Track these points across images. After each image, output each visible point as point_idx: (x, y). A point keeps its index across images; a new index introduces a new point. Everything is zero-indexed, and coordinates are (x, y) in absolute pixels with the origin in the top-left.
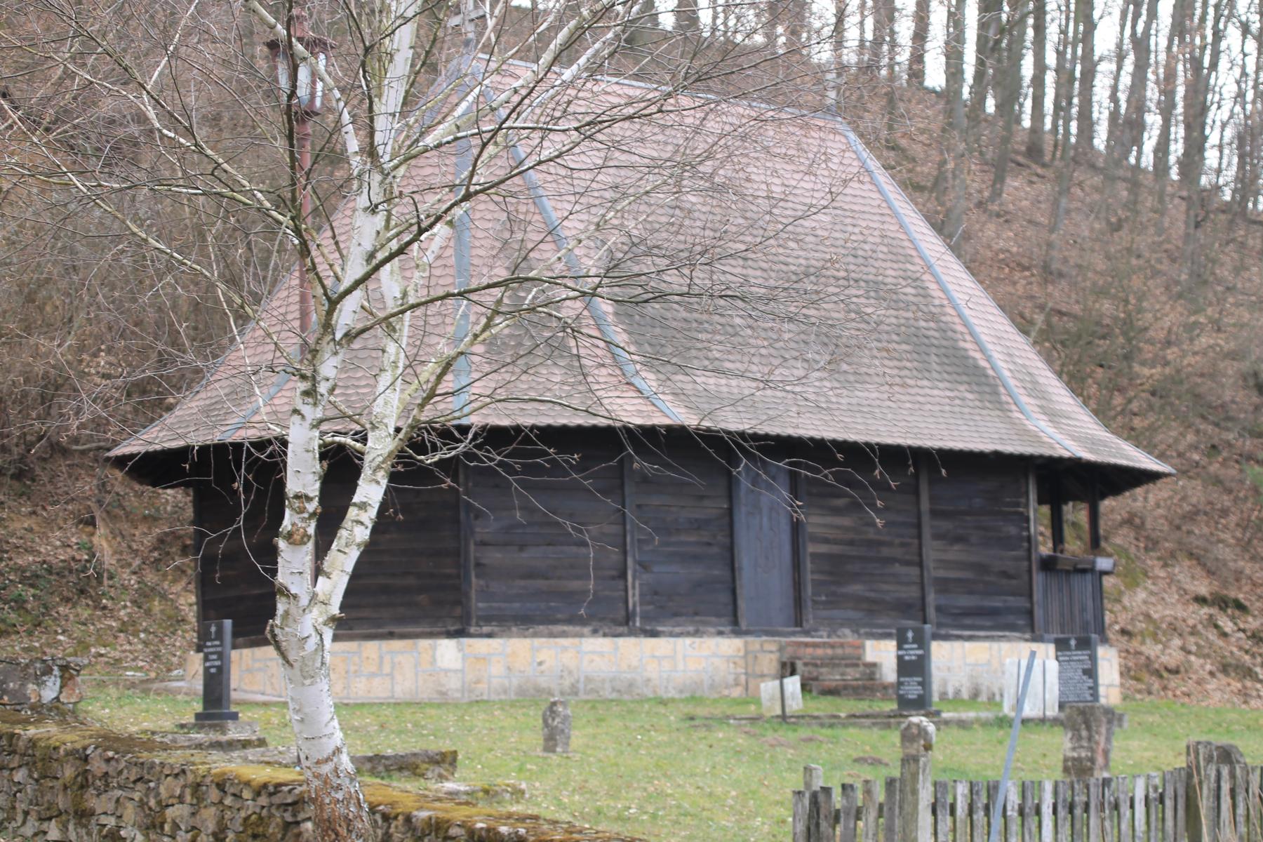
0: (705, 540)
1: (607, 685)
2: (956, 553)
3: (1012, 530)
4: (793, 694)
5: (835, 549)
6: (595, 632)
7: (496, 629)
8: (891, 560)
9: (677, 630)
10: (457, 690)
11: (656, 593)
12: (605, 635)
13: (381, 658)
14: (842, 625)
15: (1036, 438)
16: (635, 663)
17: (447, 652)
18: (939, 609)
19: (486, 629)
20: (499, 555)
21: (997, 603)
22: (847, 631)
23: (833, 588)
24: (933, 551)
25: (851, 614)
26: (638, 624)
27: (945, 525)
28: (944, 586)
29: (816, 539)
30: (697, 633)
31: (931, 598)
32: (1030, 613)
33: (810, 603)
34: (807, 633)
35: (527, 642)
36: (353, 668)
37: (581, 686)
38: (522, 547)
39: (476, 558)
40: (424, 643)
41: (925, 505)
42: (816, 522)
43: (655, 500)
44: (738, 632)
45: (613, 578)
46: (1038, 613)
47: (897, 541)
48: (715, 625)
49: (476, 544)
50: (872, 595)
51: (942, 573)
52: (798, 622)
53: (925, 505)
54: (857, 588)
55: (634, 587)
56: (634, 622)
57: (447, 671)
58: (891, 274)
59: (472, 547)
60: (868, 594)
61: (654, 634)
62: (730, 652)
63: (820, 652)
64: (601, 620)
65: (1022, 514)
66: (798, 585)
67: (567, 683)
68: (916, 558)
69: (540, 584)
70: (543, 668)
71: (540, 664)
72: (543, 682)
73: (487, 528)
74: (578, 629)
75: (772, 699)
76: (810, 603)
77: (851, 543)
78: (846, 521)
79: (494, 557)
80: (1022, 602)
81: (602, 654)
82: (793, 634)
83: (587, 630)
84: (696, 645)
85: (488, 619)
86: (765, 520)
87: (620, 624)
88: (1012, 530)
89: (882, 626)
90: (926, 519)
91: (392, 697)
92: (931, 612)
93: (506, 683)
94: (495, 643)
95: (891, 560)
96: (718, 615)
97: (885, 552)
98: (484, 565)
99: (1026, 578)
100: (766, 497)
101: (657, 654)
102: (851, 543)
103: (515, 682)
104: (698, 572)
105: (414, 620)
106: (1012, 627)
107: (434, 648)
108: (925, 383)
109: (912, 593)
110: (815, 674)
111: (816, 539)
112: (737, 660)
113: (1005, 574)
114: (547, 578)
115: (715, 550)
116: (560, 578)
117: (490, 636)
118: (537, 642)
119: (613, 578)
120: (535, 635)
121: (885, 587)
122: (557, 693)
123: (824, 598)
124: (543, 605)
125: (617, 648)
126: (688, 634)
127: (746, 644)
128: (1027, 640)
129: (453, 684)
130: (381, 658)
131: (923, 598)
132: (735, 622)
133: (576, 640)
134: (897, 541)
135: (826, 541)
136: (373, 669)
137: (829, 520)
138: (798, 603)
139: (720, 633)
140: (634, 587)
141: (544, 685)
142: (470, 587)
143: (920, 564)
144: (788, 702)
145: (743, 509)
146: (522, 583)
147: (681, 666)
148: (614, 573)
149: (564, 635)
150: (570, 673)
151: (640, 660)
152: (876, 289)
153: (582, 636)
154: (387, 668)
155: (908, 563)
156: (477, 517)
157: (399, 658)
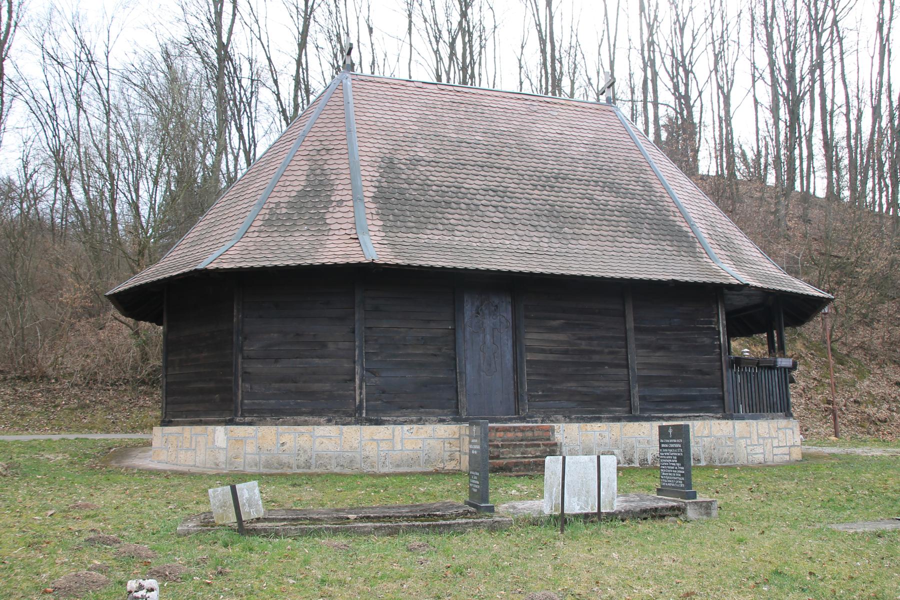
0: (431, 352)
1: (333, 461)
2: (657, 358)
3: (707, 341)
4: (249, 500)
5: (551, 357)
6: (329, 421)
7: (255, 419)
8: (602, 364)
9: (401, 419)
10: (223, 463)
11: (384, 392)
12: (337, 424)
13: (191, 438)
14: (556, 413)
15: (717, 273)
16: (355, 445)
17: (220, 434)
18: (642, 398)
19: (247, 419)
20: (260, 366)
21: (694, 392)
22: (560, 417)
23: (549, 386)
24: (637, 358)
25: (564, 404)
26: (364, 415)
27: (650, 338)
28: (646, 381)
29: (531, 350)
30: (419, 421)
31: (636, 391)
32: (722, 398)
33: (526, 397)
34: (523, 419)
35: (274, 428)
36: (180, 444)
37: (313, 461)
38: (277, 360)
39: (243, 368)
40: (210, 428)
41: (630, 324)
42: (533, 337)
43: (385, 324)
44: (458, 420)
45: (346, 381)
46: (728, 398)
47: (606, 350)
48: (433, 414)
49: (243, 358)
50: (585, 389)
51: (645, 373)
52: (517, 413)
53: (630, 324)
54: (571, 385)
55: (361, 388)
56: (361, 414)
57: (220, 448)
58: (624, 178)
59: (240, 360)
60: (580, 389)
61: (378, 423)
62: (446, 435)
63: (510, 435)
64: (335, 412)
65: (714, 328)
66: (517, 384)
67: (302, 459)
68: (624, 362)
69: (291, 386)
70: (285, 447)
71: (283, 444)
72: (284, 458)
73: (251, 348)
74: (316, 419)
75: (223, 505)
76: (526, 397)
77: (566, 352)
78: (562, 337)
79: (255, 367)
80: (716, 391)
81: (330, 438)
82: (510, 420)
83: (322, 420)
84: (414, 431)
85: (251, 412)
86: (488, 337)
87: (351, 416)
88: (707, 341)
89: (593, 412)
90: (631, 335)
91: (195, 466)
92: (636, 401)
93: (257, 457)
94: (250, 429)
95: (602, 364)
96: (442, 407)
97: (596, 358)
98: (249, 373)
99: (719, 374)
100: (488, 322)
101: (375, 438)
102: (566, 352)
103: (263, 457)
104: (424, 375)
105: (207, 413)
106: (707, 410)
107: (214, 432)
108: (634, 240)
109: (621, 387)
110: (496, 454)
111: (531, 350)
112: (451, 441)
113: (701, 372)
114: (295, 382)
115: (440, 359)
116: (305, 382)
117: (250, 424)
118: (281, 428)
119: (346, 381)
120: (283, 424)
121: (596, 384)
122: (294, 466)
123: (540, 393)
124: (292, 402)
125: (341, 434)
126: (411, 422)
127: (460, 428)
128: (719, 418)
129: (222, 458)
130: (191, 438)
131: (629, 391)
132: (457, 413)
133: (310, 428)
134: (606, 350)
135: (542, 351)
136: (188, 445)
137: (546, 336)
138: (518, 397)
139: (442, 421)
140: (361, 388)
141: (286, 461)
142: (238, 390)
143: (627, 367)
144: (244, 509)
145: (468, 329)
146: (277, 385)
147: (398, 446)
148: (347, 378)
149: (305, 423)
150: (305, 451)
151: (360, 442)
152: (612, 187)
153: (319, 424)
154: (193, 447)
155: (618, 366)
156: (245, 338)
157: (199, 439)
